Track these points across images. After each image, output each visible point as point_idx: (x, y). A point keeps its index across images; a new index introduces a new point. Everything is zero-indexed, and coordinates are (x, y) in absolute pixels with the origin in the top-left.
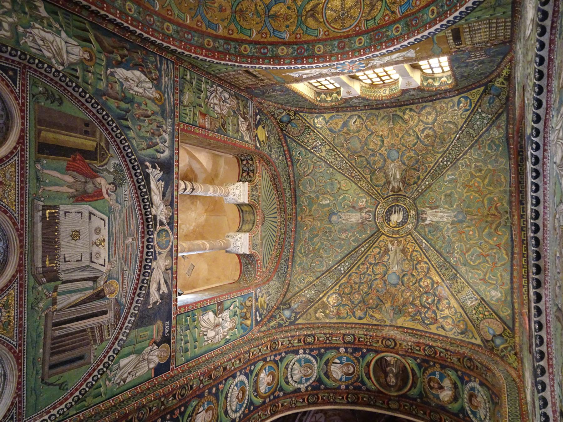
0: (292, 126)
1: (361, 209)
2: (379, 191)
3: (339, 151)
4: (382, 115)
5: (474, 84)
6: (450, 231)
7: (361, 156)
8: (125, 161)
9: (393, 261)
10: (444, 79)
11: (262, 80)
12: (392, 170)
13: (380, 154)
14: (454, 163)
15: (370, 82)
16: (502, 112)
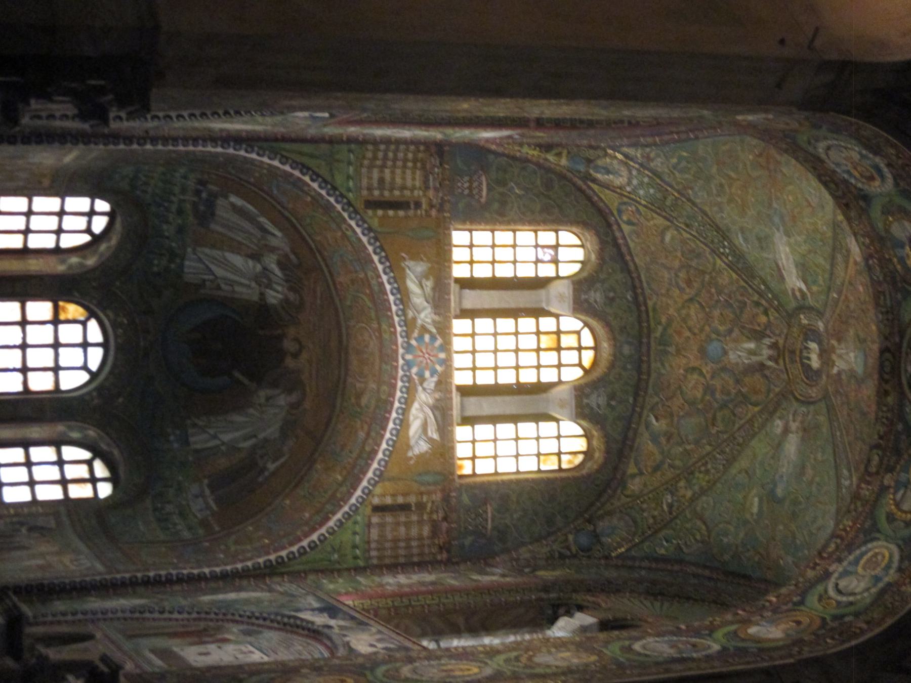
0: (608, 535)
1: (786, 431)
2: (777, 390)
3: (696, 462)
4: (659, 365)
5: (589, 199)
6: (799, 239)
7: (714, 418)
8: (253, 624)
9: (847, 362)
10: (589, 246)
11: (421, 506)
12: (740, 356)
13: (712, 377)
14: (723, 234)
15: (579, 373)
16: (622, 154)
